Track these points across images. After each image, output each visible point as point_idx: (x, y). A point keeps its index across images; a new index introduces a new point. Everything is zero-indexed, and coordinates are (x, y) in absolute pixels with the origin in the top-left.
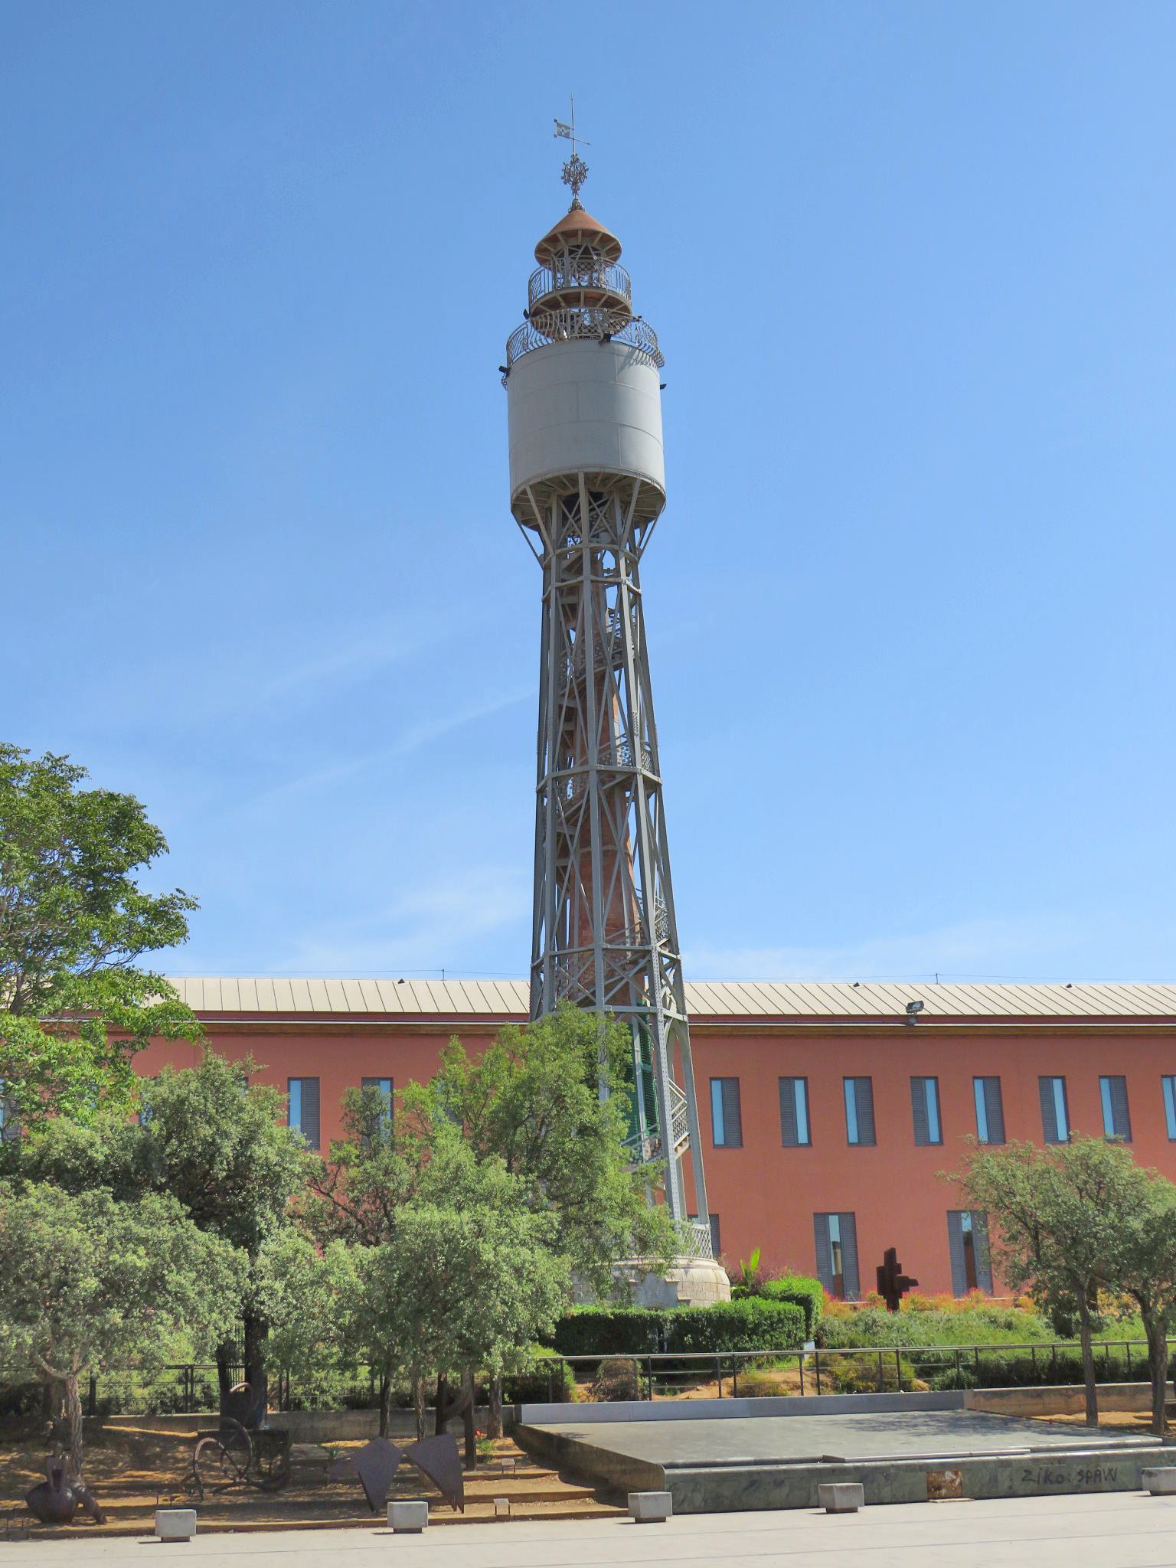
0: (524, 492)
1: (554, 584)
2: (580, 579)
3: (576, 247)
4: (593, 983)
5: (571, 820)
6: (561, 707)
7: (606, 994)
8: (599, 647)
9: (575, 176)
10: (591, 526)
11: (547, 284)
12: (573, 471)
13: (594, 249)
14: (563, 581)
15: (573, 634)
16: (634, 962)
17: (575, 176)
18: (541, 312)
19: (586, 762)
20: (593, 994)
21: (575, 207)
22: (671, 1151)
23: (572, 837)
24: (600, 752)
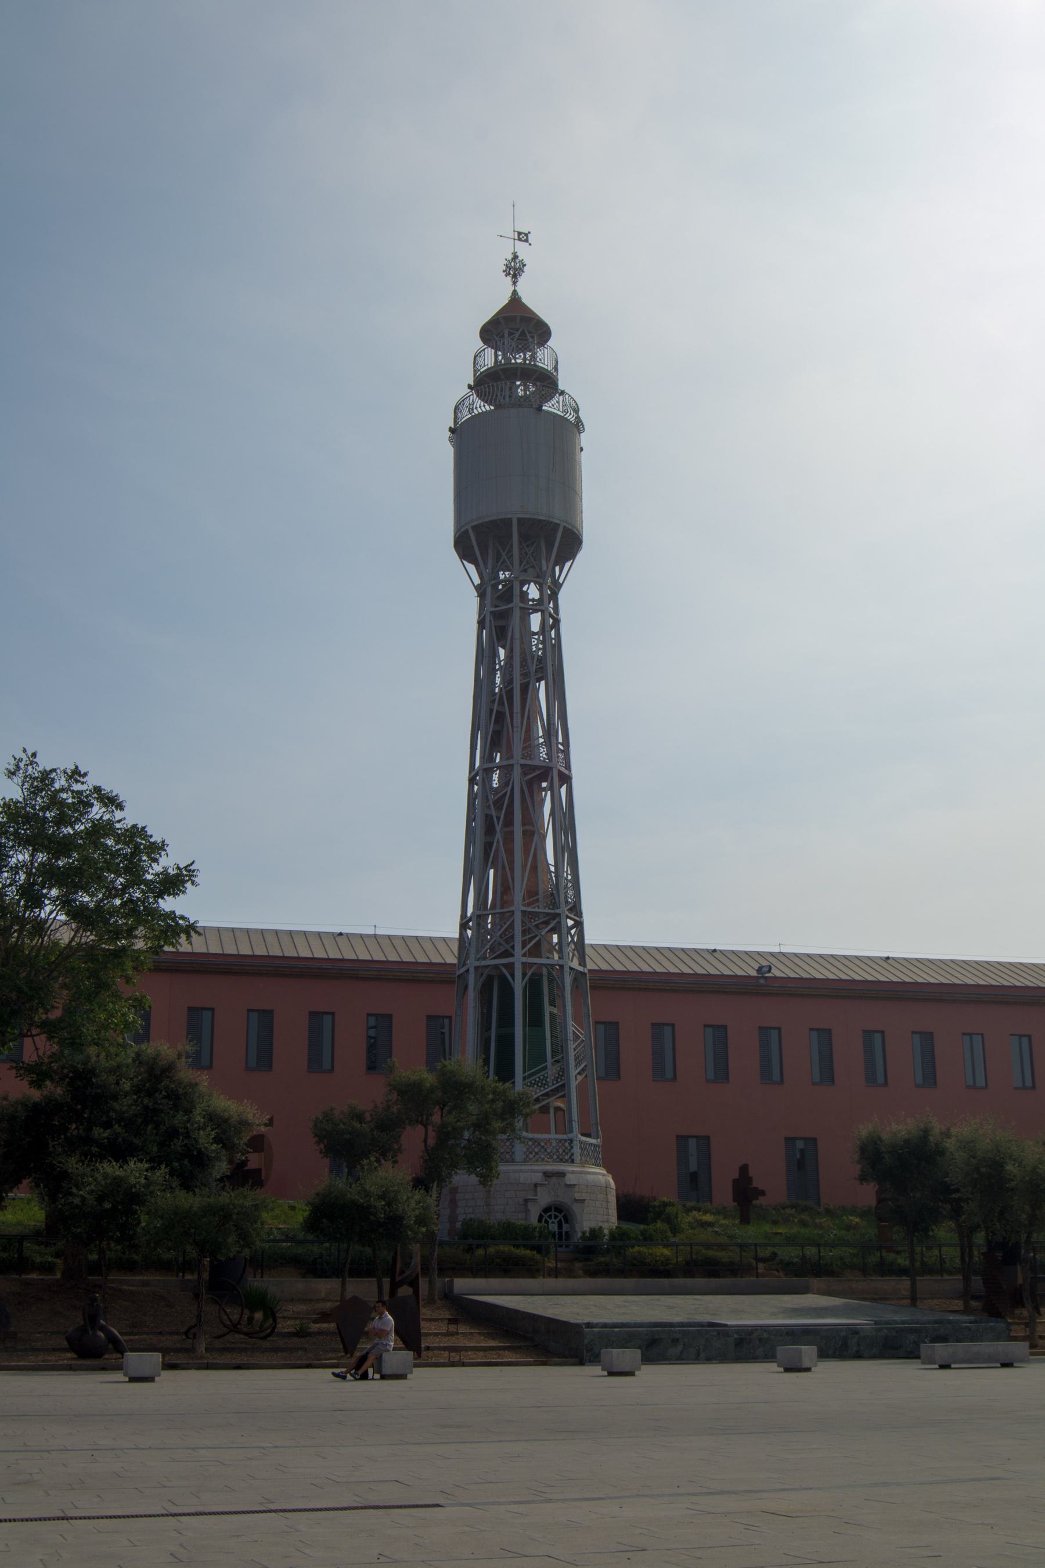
1: (489, 608)
2: (510, 606)
3: (515, 328)
4: (512, 937)
5: (498, 804)
6: (491, 710)
7: (523, 947)
8: (524, 663)
9: (514, 269)
10: (521, 562)
12: (509, 516)
13: (530, 332)
14: (496, 606)
15: (502, 652)
16: (547, 923)
17: (514, 269)
19: (512, 757)
20: (513, 947)
21: (515, 292)
22: (572, 1078)
23: (498, 818)
24: (524, 749)
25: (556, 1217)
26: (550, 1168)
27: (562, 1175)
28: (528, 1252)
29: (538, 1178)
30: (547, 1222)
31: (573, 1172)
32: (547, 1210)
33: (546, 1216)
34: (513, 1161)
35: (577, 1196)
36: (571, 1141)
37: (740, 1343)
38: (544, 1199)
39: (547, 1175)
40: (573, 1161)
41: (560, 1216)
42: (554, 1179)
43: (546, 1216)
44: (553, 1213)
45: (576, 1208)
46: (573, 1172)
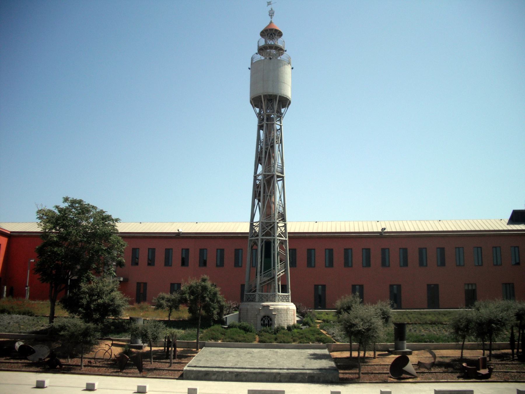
3: (270, 33)
11: (262, 42)
18: (261, 50)
21: (271, 22)
27: (268, 306)
32: (264, 317)
38: (262, 314)
44: (266, 318)
45: (272, 317)
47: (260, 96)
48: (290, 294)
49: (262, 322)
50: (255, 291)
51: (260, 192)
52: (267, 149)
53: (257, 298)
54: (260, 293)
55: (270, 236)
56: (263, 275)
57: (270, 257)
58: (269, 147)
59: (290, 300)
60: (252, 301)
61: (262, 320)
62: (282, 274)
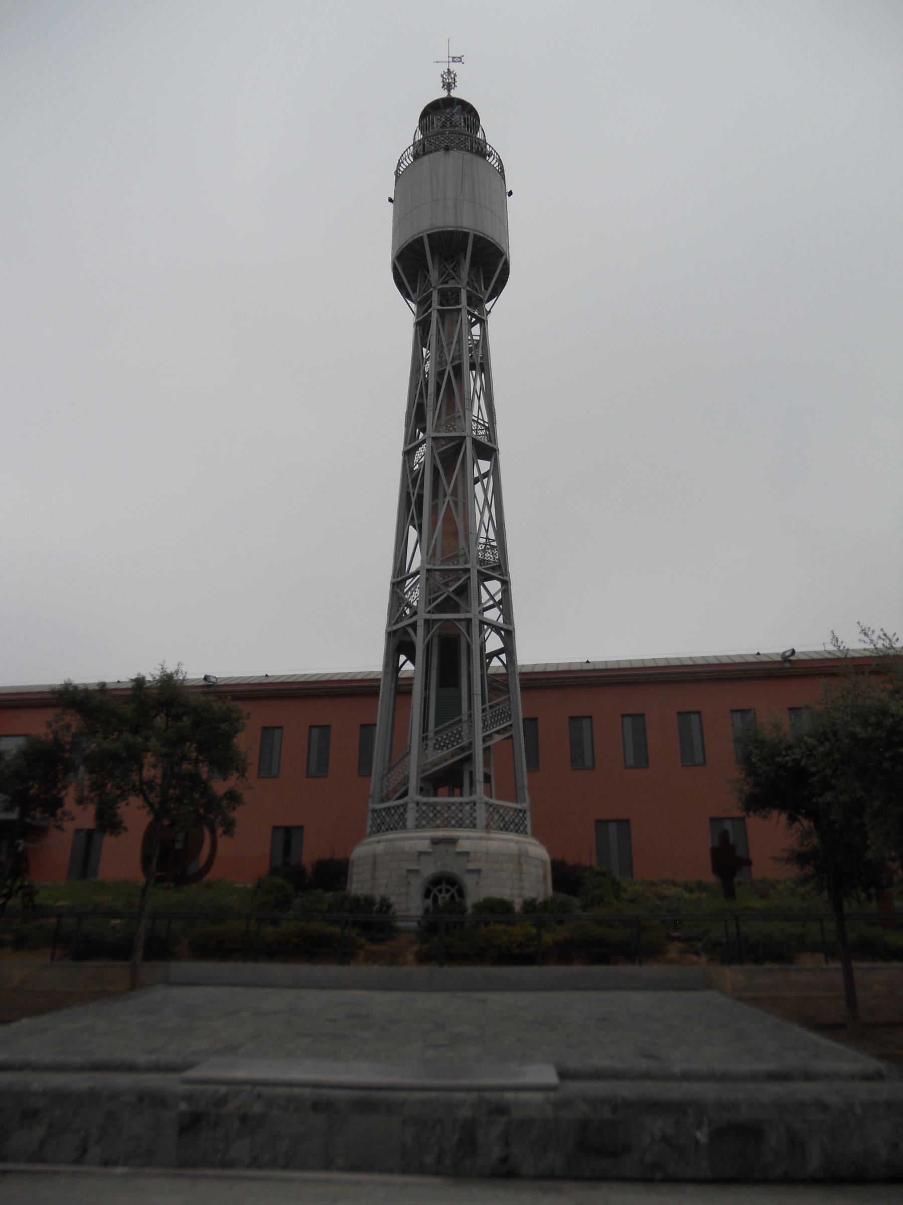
0: (419, 241)
25: (447, 891)
26: (440, 833)
27: (453, 841)
28: (336, 929)
29: (424, 845)
30: (435, 899)
31: (469, 838)
33: (435, 891)
34: (404, 827)
35: (472, 866)
36: (475, 804)
37: (192, 1123)
38: (429, 869)
39: (436, 842)
40: (475, 826)
41: (453, 890)
42: (441, 847)
43: (435, 891)
44: (444, 886)
45: (469, 882)
46: (469, 840)
47: (422, 238)
48: (525, 805)
49: (430, 902)
50: (405, 793)
51: (420, 497)
52: (440, 374)
53: (411, 816)
54: (419, 798)
55: (456, 608)
56: (431, 744)
57: (456, 684)
58: (449, 368)
59: (529, 829)
60: (394, 829)
61: (427, 894)
62: (497, 738)
